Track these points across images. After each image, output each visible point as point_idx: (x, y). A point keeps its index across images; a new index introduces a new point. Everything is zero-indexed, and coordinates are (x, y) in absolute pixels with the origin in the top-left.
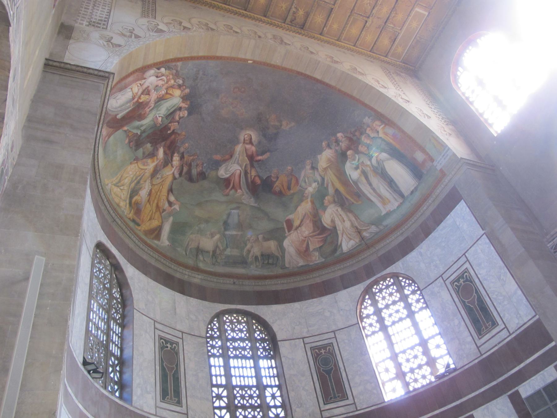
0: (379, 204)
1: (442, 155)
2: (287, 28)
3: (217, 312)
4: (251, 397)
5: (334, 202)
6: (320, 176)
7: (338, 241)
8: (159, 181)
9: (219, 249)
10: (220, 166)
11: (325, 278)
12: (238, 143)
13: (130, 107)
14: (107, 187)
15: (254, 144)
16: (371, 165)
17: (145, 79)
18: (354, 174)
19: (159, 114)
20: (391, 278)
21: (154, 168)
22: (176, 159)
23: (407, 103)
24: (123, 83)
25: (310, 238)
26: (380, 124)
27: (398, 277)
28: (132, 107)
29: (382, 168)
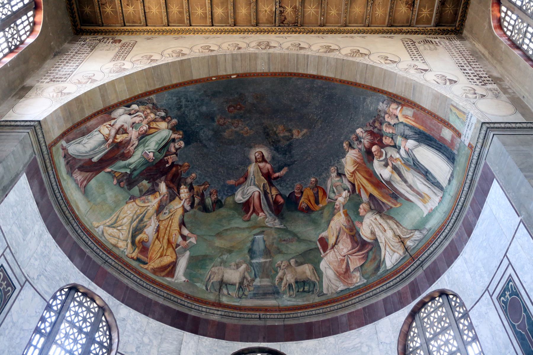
0: (419, 204)
1: (467, 125)
2: (279, 30)
3: (234, 352)
5: (371, 209)
6: (350, 182)
7: (380, 256)
8: (166, 216)
9: (247, 279)
10: (236, 190)
11: (366, 304)
12: (250, 163)
13: (107, 149)
14: (97, 230)
15: (268, 160)
16: (400, 158)
17: (114, 119)
18: (385, 173)
19: (149, 149)
20: (440, 296)
21: (158, 204)
22: (184, 191)
23: (422, 72)
24: (83, 127)
25: (350, 256)
26: (396, 107)
27: (447, 295)
28: (109, 148)
29: (413, 159)
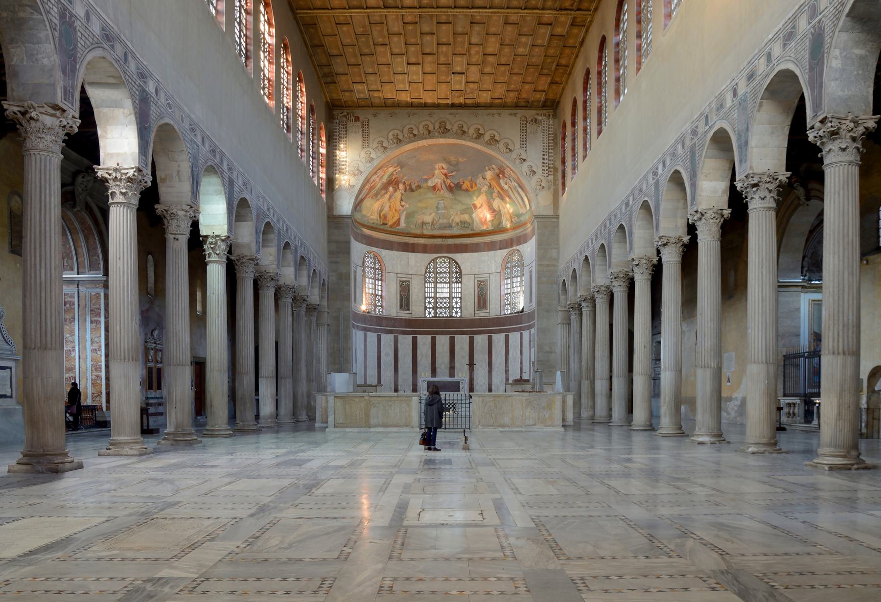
4: (445, 303)
12: (436, 169)
18: (506, 187)
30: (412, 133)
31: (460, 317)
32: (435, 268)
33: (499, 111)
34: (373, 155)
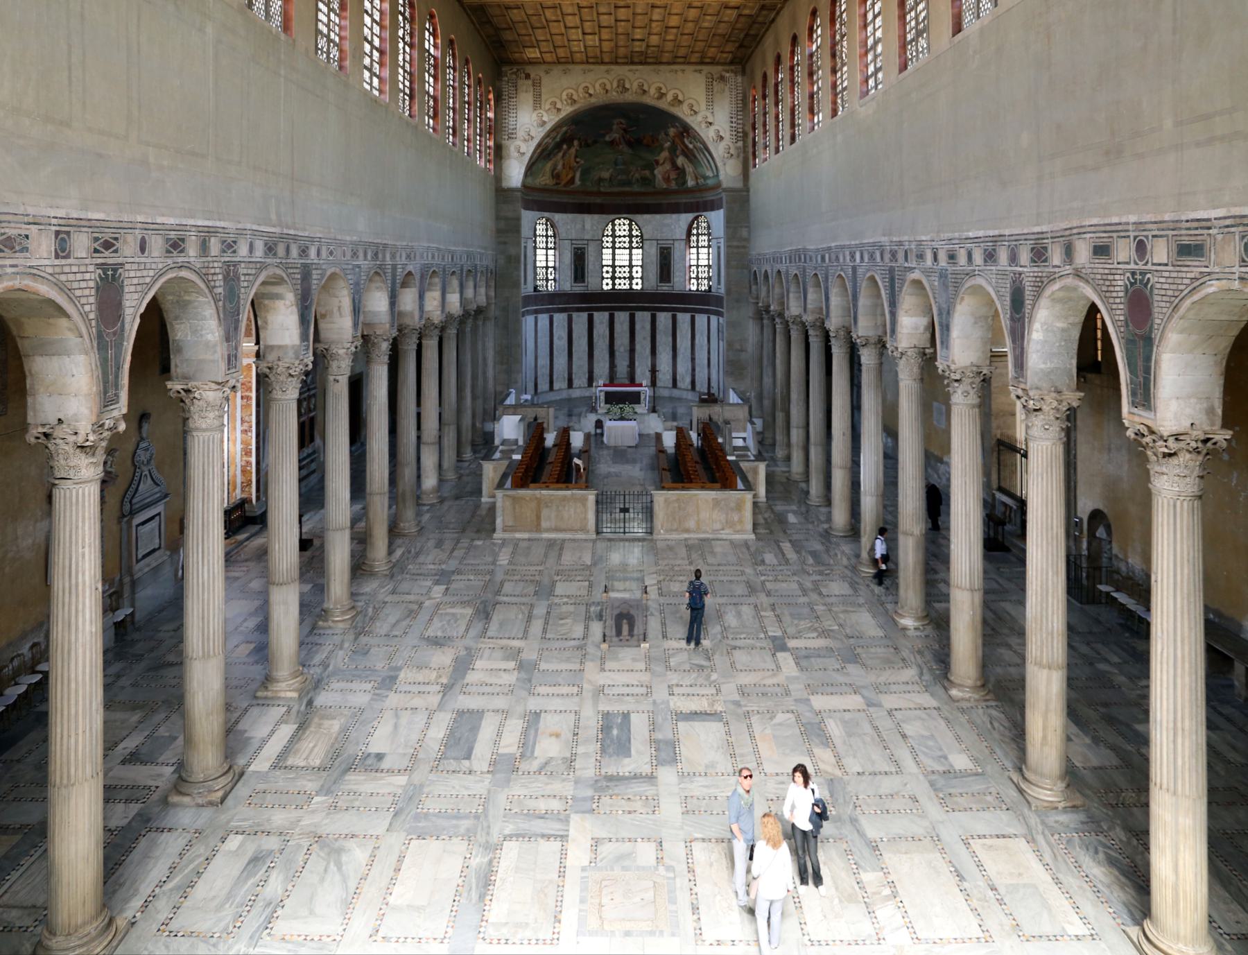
18: (691, 146)
30: (587, 93)
31: (642, 289)
32: (613, 230)
33: (682, 67)
34: (545, 118)
